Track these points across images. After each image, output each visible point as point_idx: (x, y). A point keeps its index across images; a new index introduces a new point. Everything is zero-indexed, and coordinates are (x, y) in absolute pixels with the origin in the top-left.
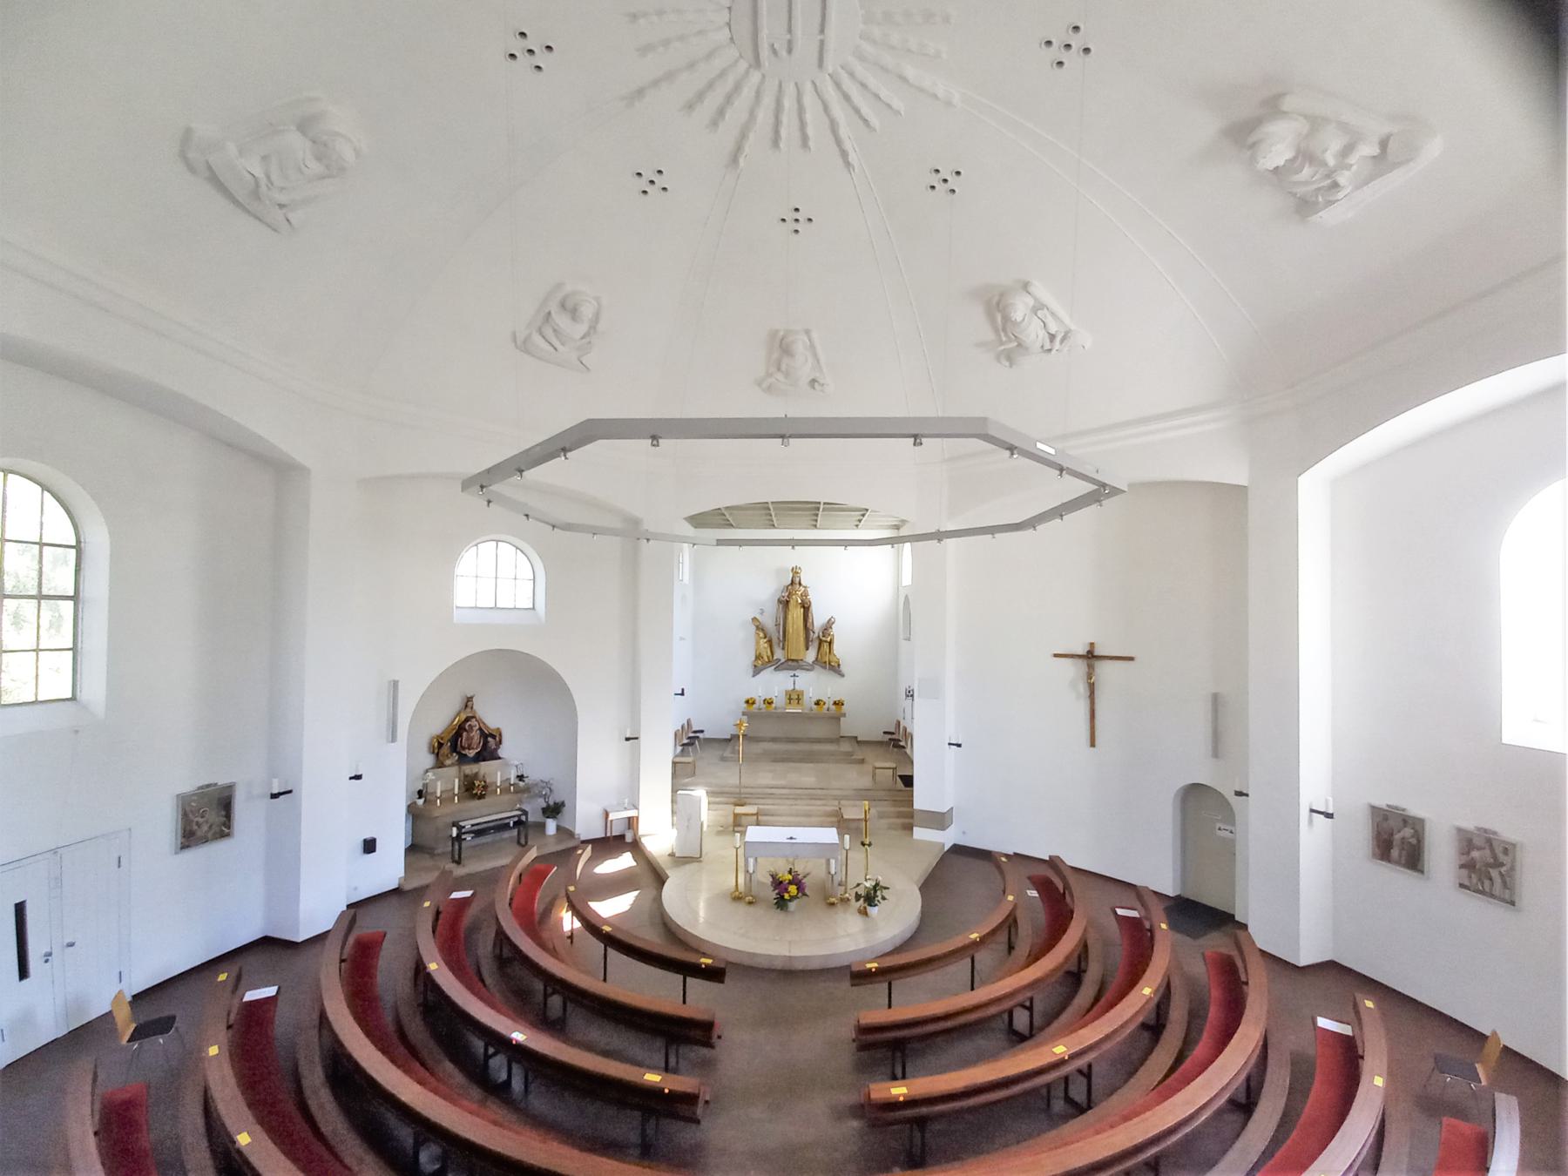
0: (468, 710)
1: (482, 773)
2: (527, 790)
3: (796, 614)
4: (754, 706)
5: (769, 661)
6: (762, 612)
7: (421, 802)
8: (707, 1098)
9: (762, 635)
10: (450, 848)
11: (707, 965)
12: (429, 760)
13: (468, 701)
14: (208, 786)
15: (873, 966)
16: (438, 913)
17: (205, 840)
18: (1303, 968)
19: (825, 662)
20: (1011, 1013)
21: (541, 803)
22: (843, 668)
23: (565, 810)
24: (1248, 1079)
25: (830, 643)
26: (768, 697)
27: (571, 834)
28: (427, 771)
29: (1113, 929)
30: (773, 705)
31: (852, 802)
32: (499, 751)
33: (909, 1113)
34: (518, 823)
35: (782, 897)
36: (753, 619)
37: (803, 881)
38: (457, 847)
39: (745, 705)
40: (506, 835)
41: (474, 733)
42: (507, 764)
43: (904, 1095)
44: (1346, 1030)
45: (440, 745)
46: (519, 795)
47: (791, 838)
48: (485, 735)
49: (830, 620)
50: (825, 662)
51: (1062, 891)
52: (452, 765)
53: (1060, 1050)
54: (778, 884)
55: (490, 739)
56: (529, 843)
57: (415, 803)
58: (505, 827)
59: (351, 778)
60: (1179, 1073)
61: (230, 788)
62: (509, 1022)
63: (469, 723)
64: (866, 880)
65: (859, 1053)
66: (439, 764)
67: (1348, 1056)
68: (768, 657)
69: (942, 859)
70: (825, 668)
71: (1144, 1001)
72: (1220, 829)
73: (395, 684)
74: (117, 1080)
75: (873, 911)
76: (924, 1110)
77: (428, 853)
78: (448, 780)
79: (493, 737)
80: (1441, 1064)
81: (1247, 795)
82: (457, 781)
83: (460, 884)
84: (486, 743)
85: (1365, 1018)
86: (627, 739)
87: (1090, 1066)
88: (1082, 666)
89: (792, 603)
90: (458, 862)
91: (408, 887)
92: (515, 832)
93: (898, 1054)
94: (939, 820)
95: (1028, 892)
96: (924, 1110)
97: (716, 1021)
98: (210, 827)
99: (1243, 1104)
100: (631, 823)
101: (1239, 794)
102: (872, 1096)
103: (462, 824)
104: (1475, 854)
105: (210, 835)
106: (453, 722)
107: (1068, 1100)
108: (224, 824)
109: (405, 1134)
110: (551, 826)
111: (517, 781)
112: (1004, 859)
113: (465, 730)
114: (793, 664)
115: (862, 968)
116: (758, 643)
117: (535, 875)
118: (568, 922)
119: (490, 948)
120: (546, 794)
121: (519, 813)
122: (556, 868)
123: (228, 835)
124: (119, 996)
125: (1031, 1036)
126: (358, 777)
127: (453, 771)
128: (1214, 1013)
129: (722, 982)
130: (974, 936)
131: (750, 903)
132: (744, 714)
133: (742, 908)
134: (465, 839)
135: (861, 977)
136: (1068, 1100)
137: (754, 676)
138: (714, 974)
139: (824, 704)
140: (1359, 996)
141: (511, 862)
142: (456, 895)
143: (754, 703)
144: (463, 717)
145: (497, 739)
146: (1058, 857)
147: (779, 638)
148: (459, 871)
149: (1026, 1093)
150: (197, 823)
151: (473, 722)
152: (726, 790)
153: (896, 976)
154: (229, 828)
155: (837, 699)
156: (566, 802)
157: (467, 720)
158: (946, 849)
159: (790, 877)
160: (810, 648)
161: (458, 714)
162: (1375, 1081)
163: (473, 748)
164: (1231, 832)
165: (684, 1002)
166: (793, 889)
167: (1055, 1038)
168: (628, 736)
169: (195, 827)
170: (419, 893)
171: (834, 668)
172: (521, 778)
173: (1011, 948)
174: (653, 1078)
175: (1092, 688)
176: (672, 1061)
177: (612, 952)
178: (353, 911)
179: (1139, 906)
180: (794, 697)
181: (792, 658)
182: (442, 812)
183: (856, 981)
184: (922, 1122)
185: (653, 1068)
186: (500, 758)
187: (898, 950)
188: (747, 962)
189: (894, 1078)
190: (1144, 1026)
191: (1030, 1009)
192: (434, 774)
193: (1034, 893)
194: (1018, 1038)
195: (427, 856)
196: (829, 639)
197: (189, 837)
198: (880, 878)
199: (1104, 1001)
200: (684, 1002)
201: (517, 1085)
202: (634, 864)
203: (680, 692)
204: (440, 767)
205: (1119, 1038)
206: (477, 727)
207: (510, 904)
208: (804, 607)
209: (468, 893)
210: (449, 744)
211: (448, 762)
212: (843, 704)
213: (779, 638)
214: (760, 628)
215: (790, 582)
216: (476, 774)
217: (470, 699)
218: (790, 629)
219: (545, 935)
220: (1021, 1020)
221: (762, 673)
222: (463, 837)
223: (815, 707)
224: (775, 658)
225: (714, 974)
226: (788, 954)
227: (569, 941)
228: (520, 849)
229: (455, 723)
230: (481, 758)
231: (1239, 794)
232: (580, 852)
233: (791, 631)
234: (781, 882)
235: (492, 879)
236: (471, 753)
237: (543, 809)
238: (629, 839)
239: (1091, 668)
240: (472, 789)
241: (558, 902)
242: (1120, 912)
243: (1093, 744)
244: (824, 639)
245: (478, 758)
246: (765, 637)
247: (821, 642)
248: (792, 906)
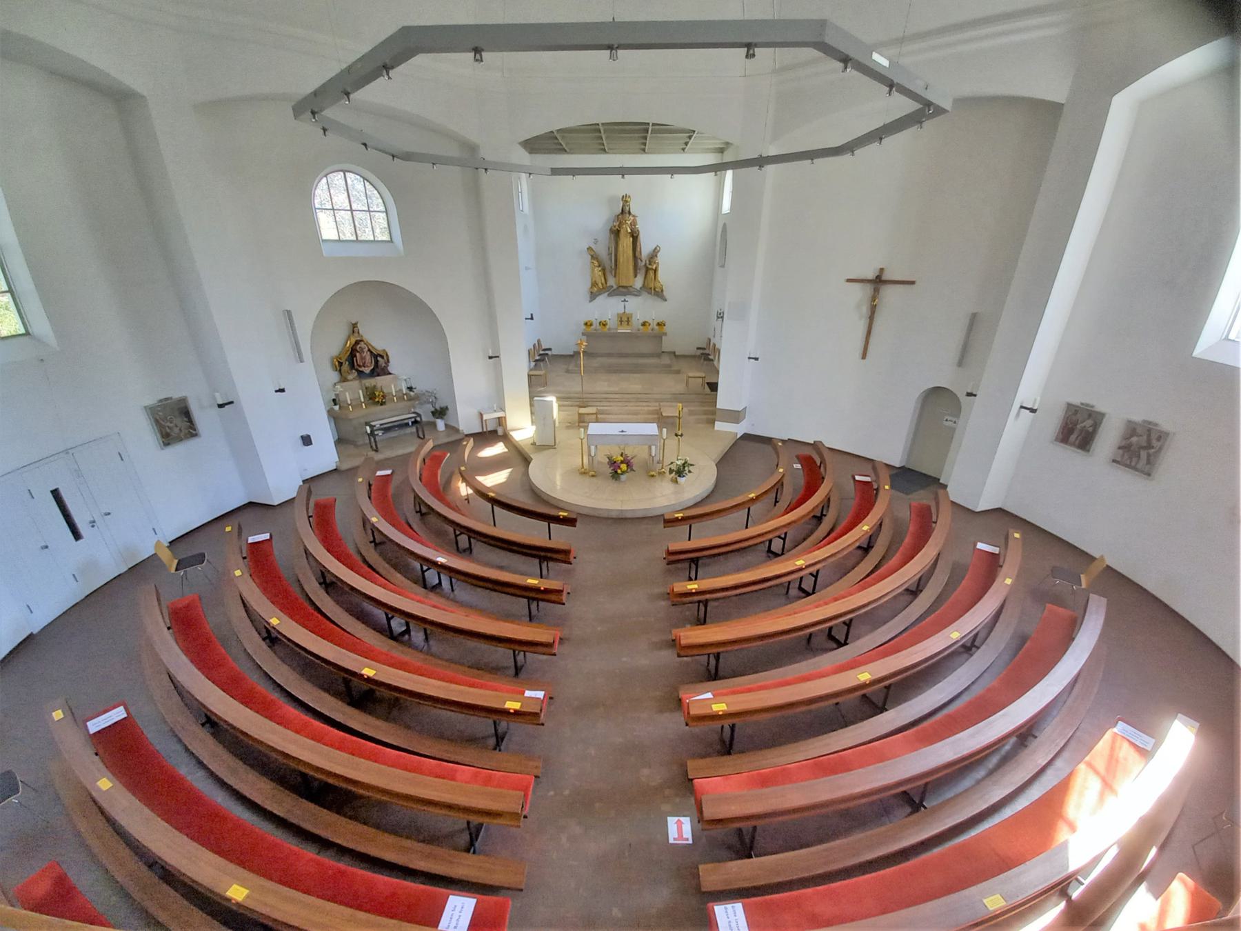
0: (356, 334)
1: (379, 385)
2: (417, 398)
3: (626, 242)
4: (592, 327)
5: (603, 288)
6: (596, 241)
7: (337, 408)
8: (569, 591)
9: (596, 264)
10: (368, 441)
11: (564, 517)
12: (334, 376)
13: (354, 327)
14: (166, 399)
15: (680, 515)
16: (370, 485)
17: (179, 439)
18: (979, 512)
19: (651, 288)
20: (770, 541)
21: (431, 408)
22: (665, 293)
23: (450, 412)
24: (920, 579)
25: (655, 271)
26: (603, 320)
27: (457, 430)
28: (335, 384)
29: (851, 487)
30: (607, 327)
31: (668, 404)
32: (389, 368)
33: (696, 598)
34: (415, 422)
35: (616, 472)
36: (588, 249)
37: (632, 461)
38: (372, 440)
39: (584, 327)
40: (408, 430)
41: (365, 353)
42: (397, 378)
43: (696, 589)
44: (996, 550)
45: (341, 364)
46: (412, 402)
47: (623, 431)
48: (376, 356)
50: (651, 288)
51: (819, 464)
53: (800, 563)
54: (613, 463)
55: (379, 359)
56: (426, 436)
57: (333, 409)
58: (407, 424)
59: (276, 391)
60: (875, 575)
61: (183, 400)
62: (435, 552)
63: (359, 346)
64: (678, 460)
65: (667, 566)
66: (344, 379)
67: (992, 564)
68: (602, 284)
69: (734, 445)
70: (651, 294)
71: (863, 533)
72: (947, 420)
73: (289, 312)
74: (174, 594)
75: (681, 480)
76: (708, 596)
77: (352, 444)
78: (353, 391)
79: (382, 357)
80: (1055, 572)
81: (975, 395)
82: (361, 392)
83: (381, 465)
84: (377, 362)
85: (1011, 543)
86: (490, 358)
87: (818, 571)
88: (869, 289)
90: (376, 451)
91: (345, 467)
92: (414, 429)
93: (693, 566)
94: (735, 416)
95: (794, 465)
96: (708, 596)
97: (572, 549)
98: (180, 430)
99: (913, 592)
100: (501, 421)
101: (969, 394)
102: (675, 590)
103: (373, 424)
104: (1134, 439)
105: (182, 435)
106: (347, 342)
107: (800, 588)
108: (191, 428)
109: (380, 614)
110: (441, 424)
111: (408, 392)
112: (780, 444)
113: (358, 352)
114: (623, 291)
115: (671, 517)
116: (593, 270)
117: (434, 460)
118: (464, 490)
119: (412, 506)
120: (432, 401)
121: (414, 415)
122: (449, 454)
123: (196, 435)
124: (158, 544)
125: (783, 554)
126: (282, 390)
127: (356, 383)
128: (908, 540)
129: (575, 526)
130: (752, 495)
131: (593, 476)
132: (583, 334)
133: (587, 480)
134: (378, 435)
135: (671, 522)
136: (800, 588)
137: (590, 301)
138: (570, 522)
139: (650, 325)
140: (1011, 531)
141: (416, 450)
142: (379, 473)
143: (591, 325)
144: (353, 340)
145: (385, 358)
146: (821, 442)
147: (611, 267)
148: (378, 457)
149: (777, 585)
150: (168, 427)
151: (362, 345)
152: (572, 395)
153: (695, 521)
154: (195, 430)
155: (660, 321)
156: (449, 407)
157: (357, 343)
158: (738, 436)
159: (622, 459)
160: (638, 276)
161: (349, 338)
162: (1006, 580)
163: (368, 366)
164: (955, 422)
165: (550, 539)
166: (624, 467)
167: (798, 557)
168: (490, 355)
169: (168, 430)
170: (353, 471)
171: (659, 294)
172: (410, 389)
173: (776, 502)
174: (532, 582)
175: (873, 310)
176: (545, 572)
177: (497, 509)
178: (307, 485)
179: (873, 475)
180: (625, 319)
181: (623, 285)
182: (353, 414)
183: (670, 524)
184: (706, 603)
185: (532, 576)
186: (390, 374)
187: (696, 505)
188: (592, 513)
189: (690, 579)
190: (859, 547)
191: (784, 539)
192: (342, 387)
193: (799, 466)
194: (772, 554)
195: (352, 446)
196: (654, 267)
197: (167, 438)
198: (688, 459)
199: (832, 535)
200: (550, 539)
201: (446, 584)
202: (506, 450)
203: (530, 317)
204: (344, 381)
205: (840, 556)
206: (367, 349)
207: (420, 479)
208: (633, 236)
209: (389, 472)
210: (347, 363)
211: (350, 377)
212: (664, 325)
213: (611, 267)
215: (621, 211)
216: (375, 386)
217: (354, 326)
218: (621, 259)
219: (449, 498)
220: (777, 545)
222: (376, 433)
223: (642, 327)
224: (608, 285)
225: (570, 522)
226: (620, 508)
227: (467, 501)
228: (420, 441)
229: (348, 345)
230: (375, 374)
231: (969, 394)
232: (465, 443)
233: (621, 260)
234: (615, 462)
235: (406, 459)
236: (367, 370)
237: (432, 412)
238: (500, 432)
239: (876, 291)
240: (374, 397)
241: (454, 477)
242: (857, 478)
243: (864, 356)
244: (650, 267)
245: (373, 373)
246: (599, 266)
247: (647, 270)
248: (623, 477)
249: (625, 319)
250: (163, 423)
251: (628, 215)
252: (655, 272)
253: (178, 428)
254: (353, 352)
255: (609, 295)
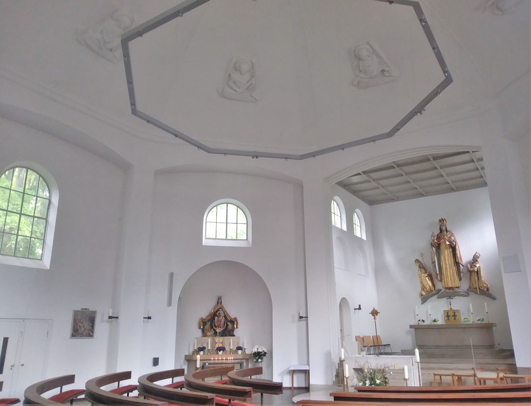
0: (219, 305)
3: (447, 253)
6: (422, 255)
12: (199, 333)
13: (219, 299)
14: (86, 309)
17: (82, 335)
19: (476, 288)
22: (491, 291)
25: (478, 273)
41: (221, 317)
49: (475, 254)
50: (476, 288)
52: (211, 335)
61: (94, 312)
63: (219, 312)
66: (204, 334)
70: (476, 293)
89: (443, 246)
105: (84, 333)
123: (92, 336)
126: (149, 318)
137: (422, 304)
150: (80, 325)
154: (92, 333)
161: (215, 307)
169: (78, 328)
196: (476, 269)
197: (76, 333)
203: (358, 308)
211: (209, 334)
214: (422, 267)
215: (439, 231)
217: (220, 298)
221: (428, 301)
229: (212, 312)
244: (472, 269)
246: (426, 273)
249: (451, 314)
250: (78, 323)
251: (446, 233)
252: (477, 274)
253: (84, 328)
254: (214, 315)
255: (438, 298)
